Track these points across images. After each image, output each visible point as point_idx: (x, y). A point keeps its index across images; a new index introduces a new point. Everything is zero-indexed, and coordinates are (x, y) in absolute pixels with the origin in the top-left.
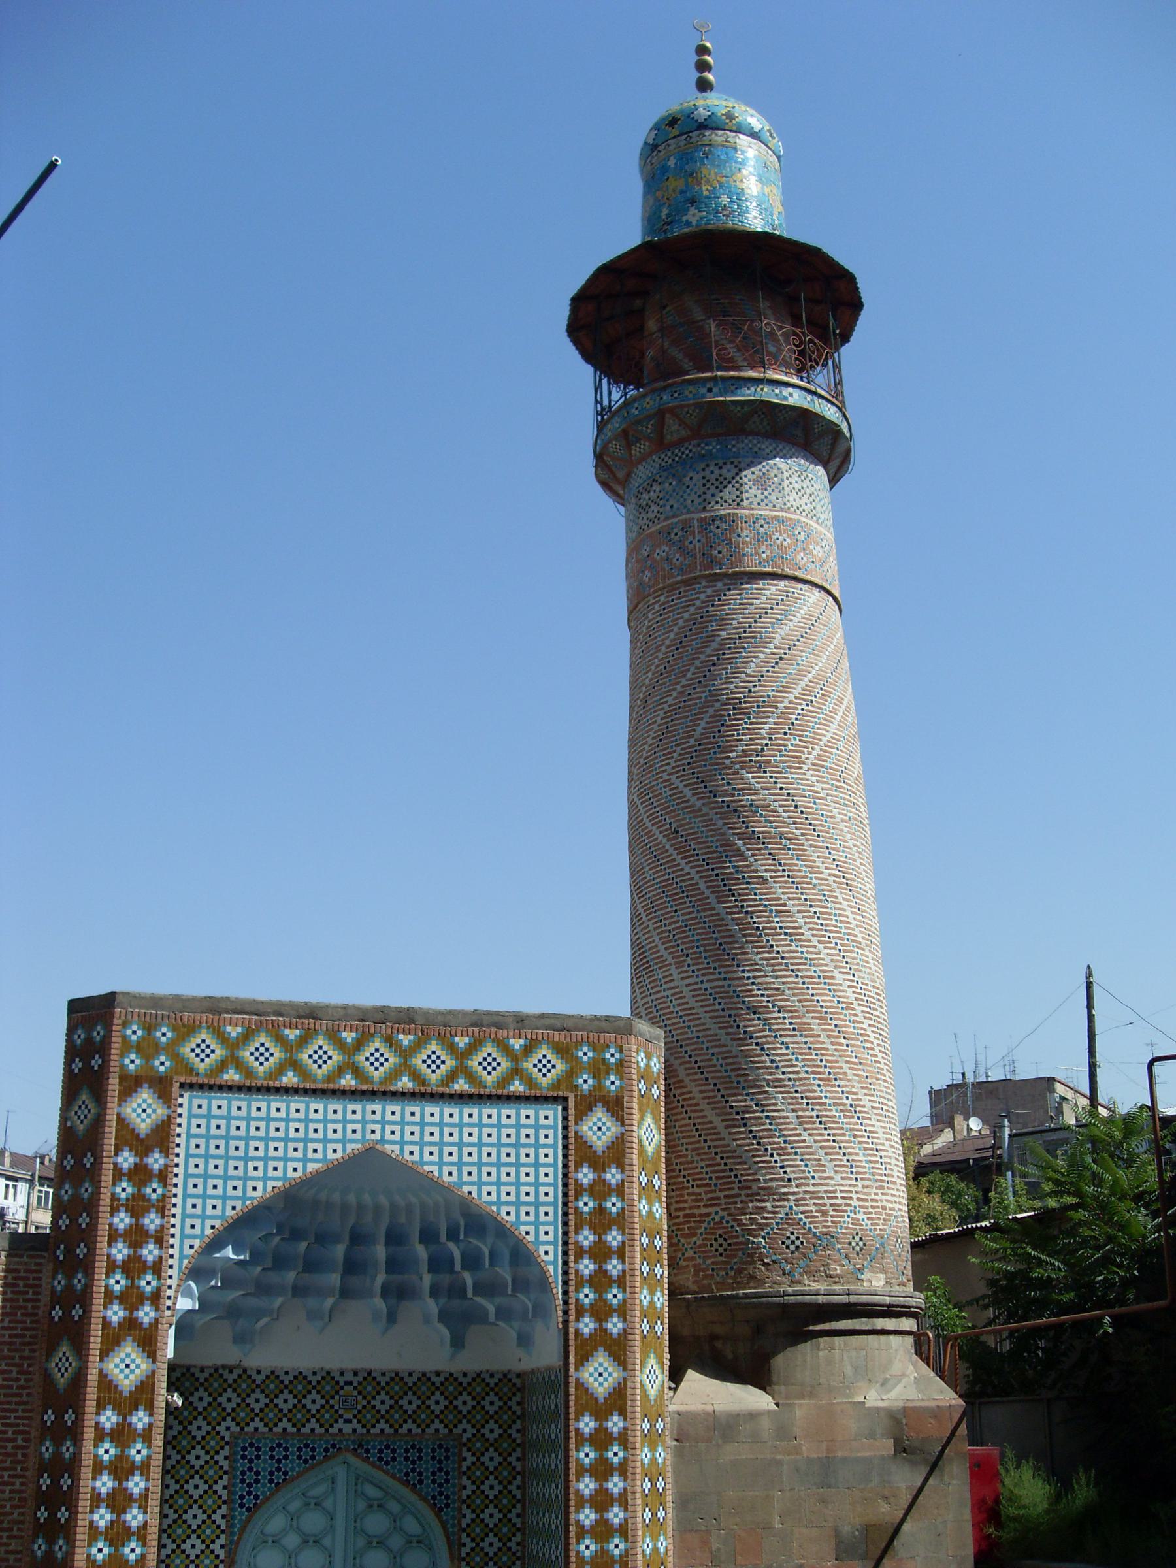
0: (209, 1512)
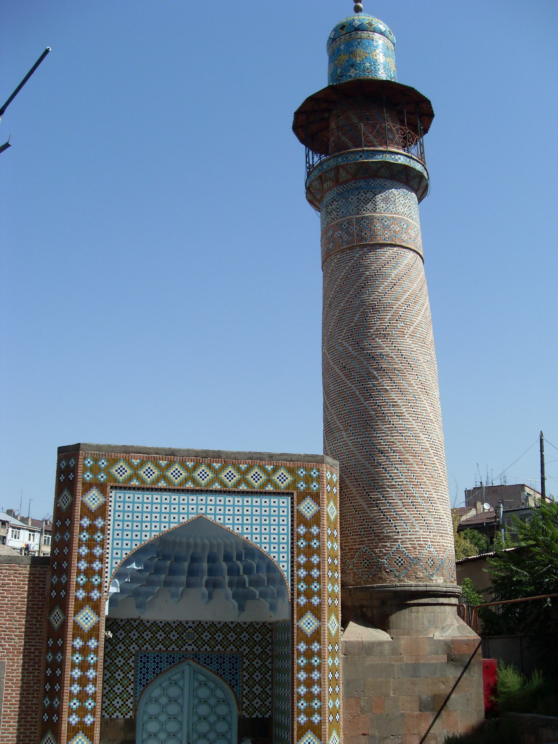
0: (125, 687)
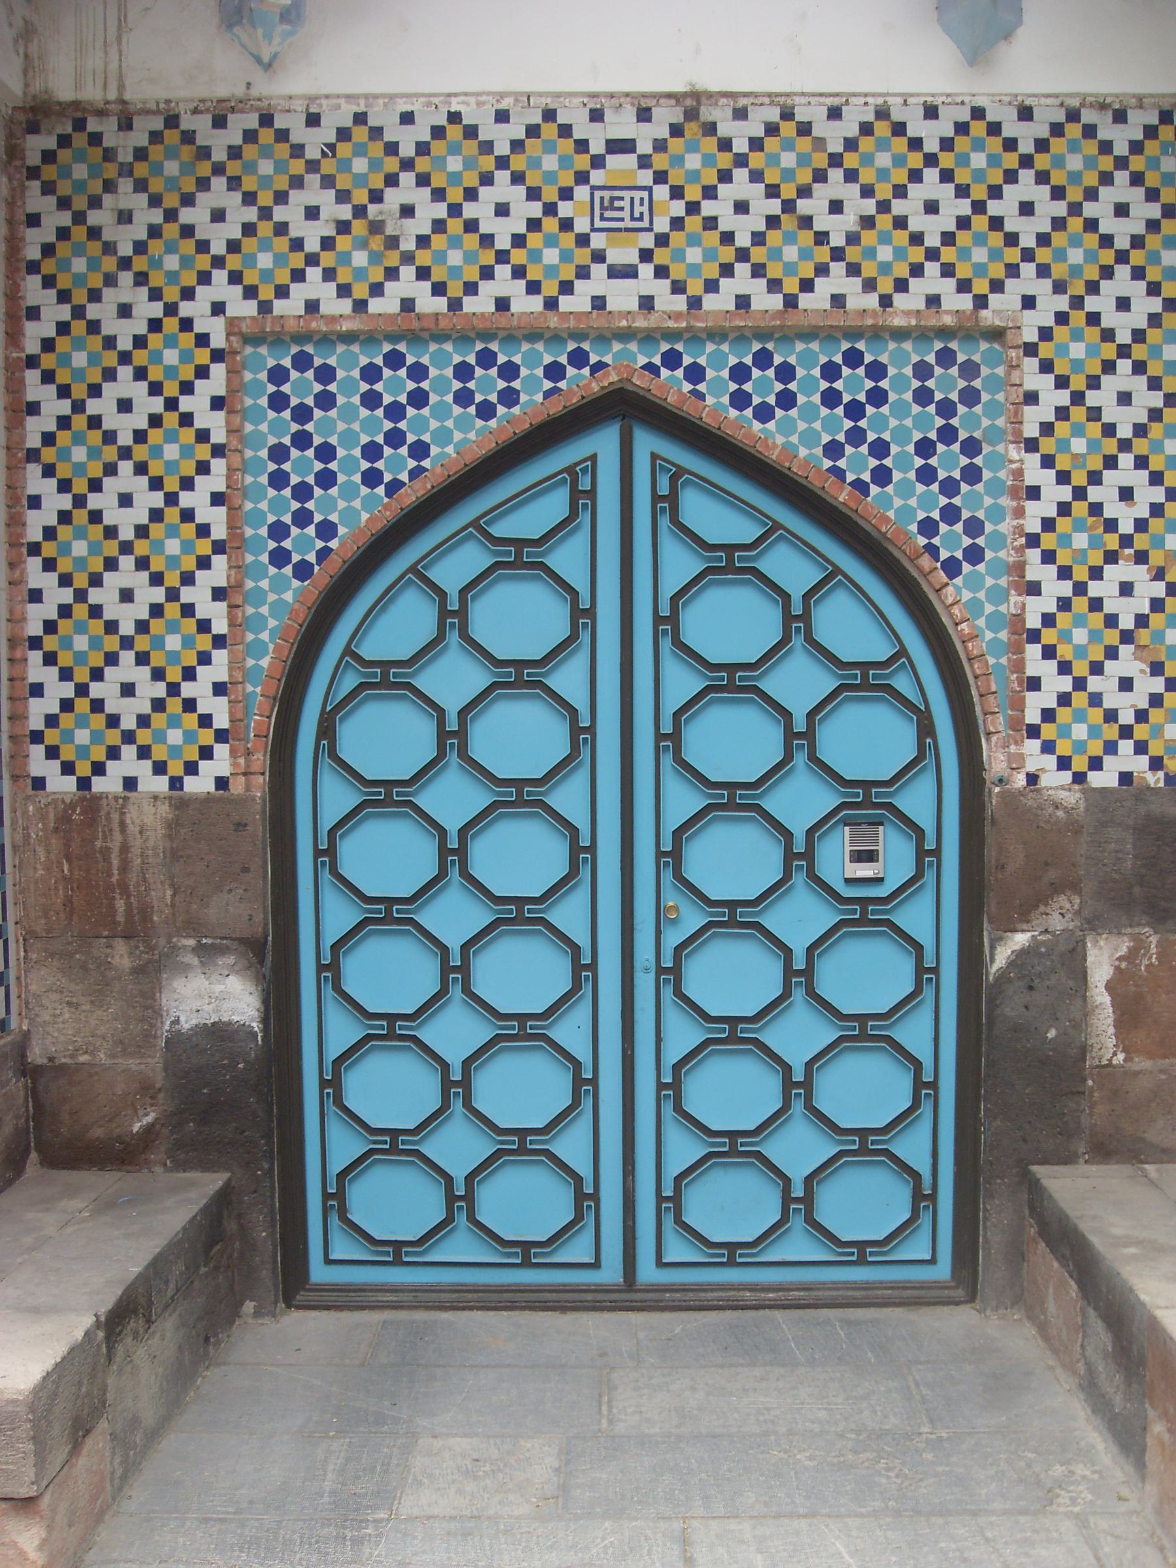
0: (172, 579)
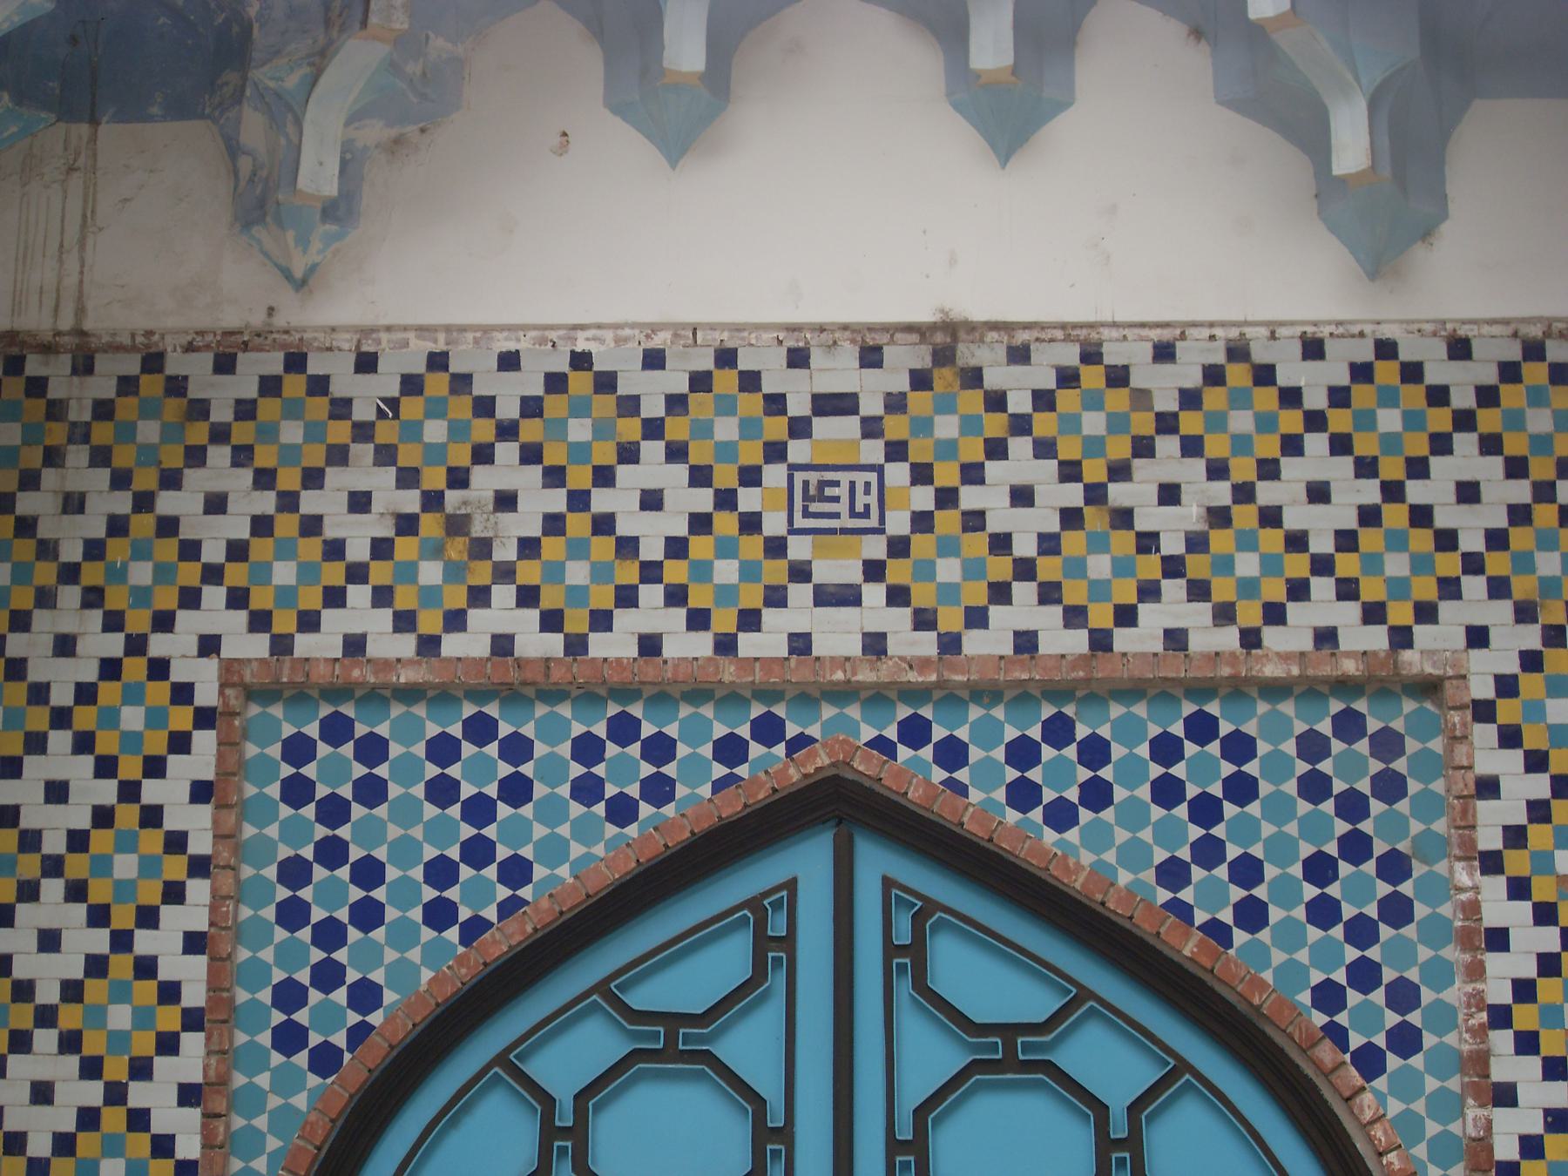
0: (116, 1069)
